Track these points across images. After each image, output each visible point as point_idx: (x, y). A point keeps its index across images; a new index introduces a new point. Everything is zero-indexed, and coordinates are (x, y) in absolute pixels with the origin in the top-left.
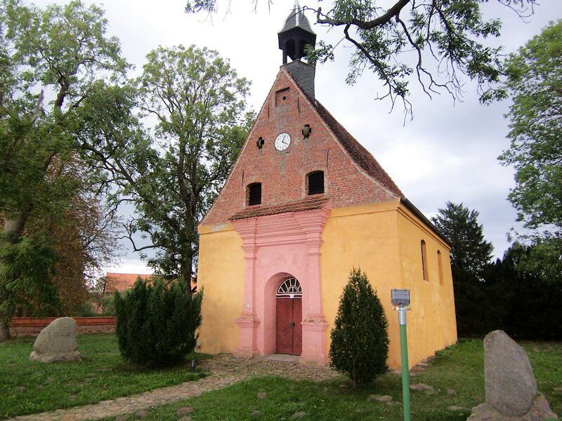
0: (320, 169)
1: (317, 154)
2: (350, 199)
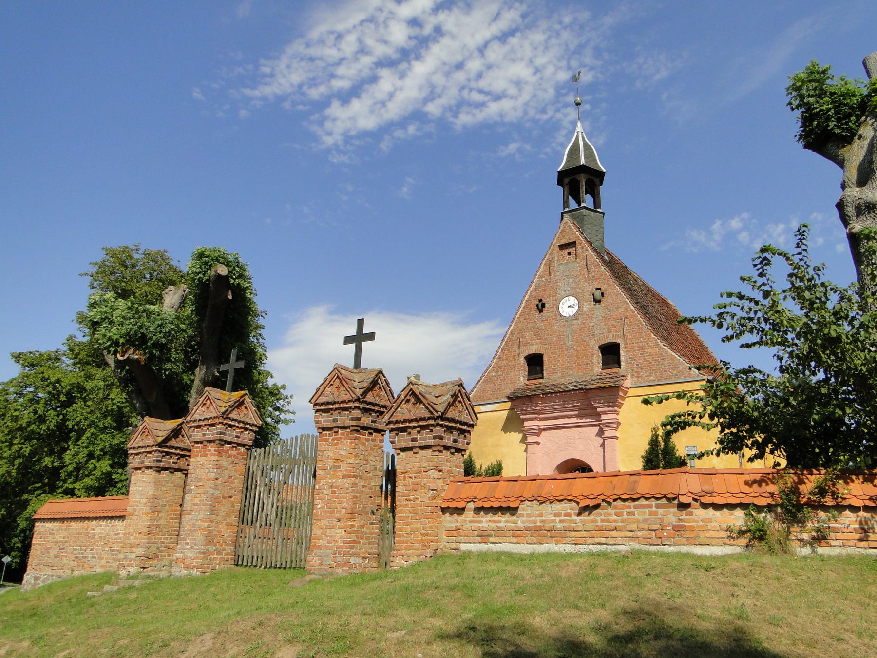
0: (614, 341)
1: (611, 323)
2: (650, 376)
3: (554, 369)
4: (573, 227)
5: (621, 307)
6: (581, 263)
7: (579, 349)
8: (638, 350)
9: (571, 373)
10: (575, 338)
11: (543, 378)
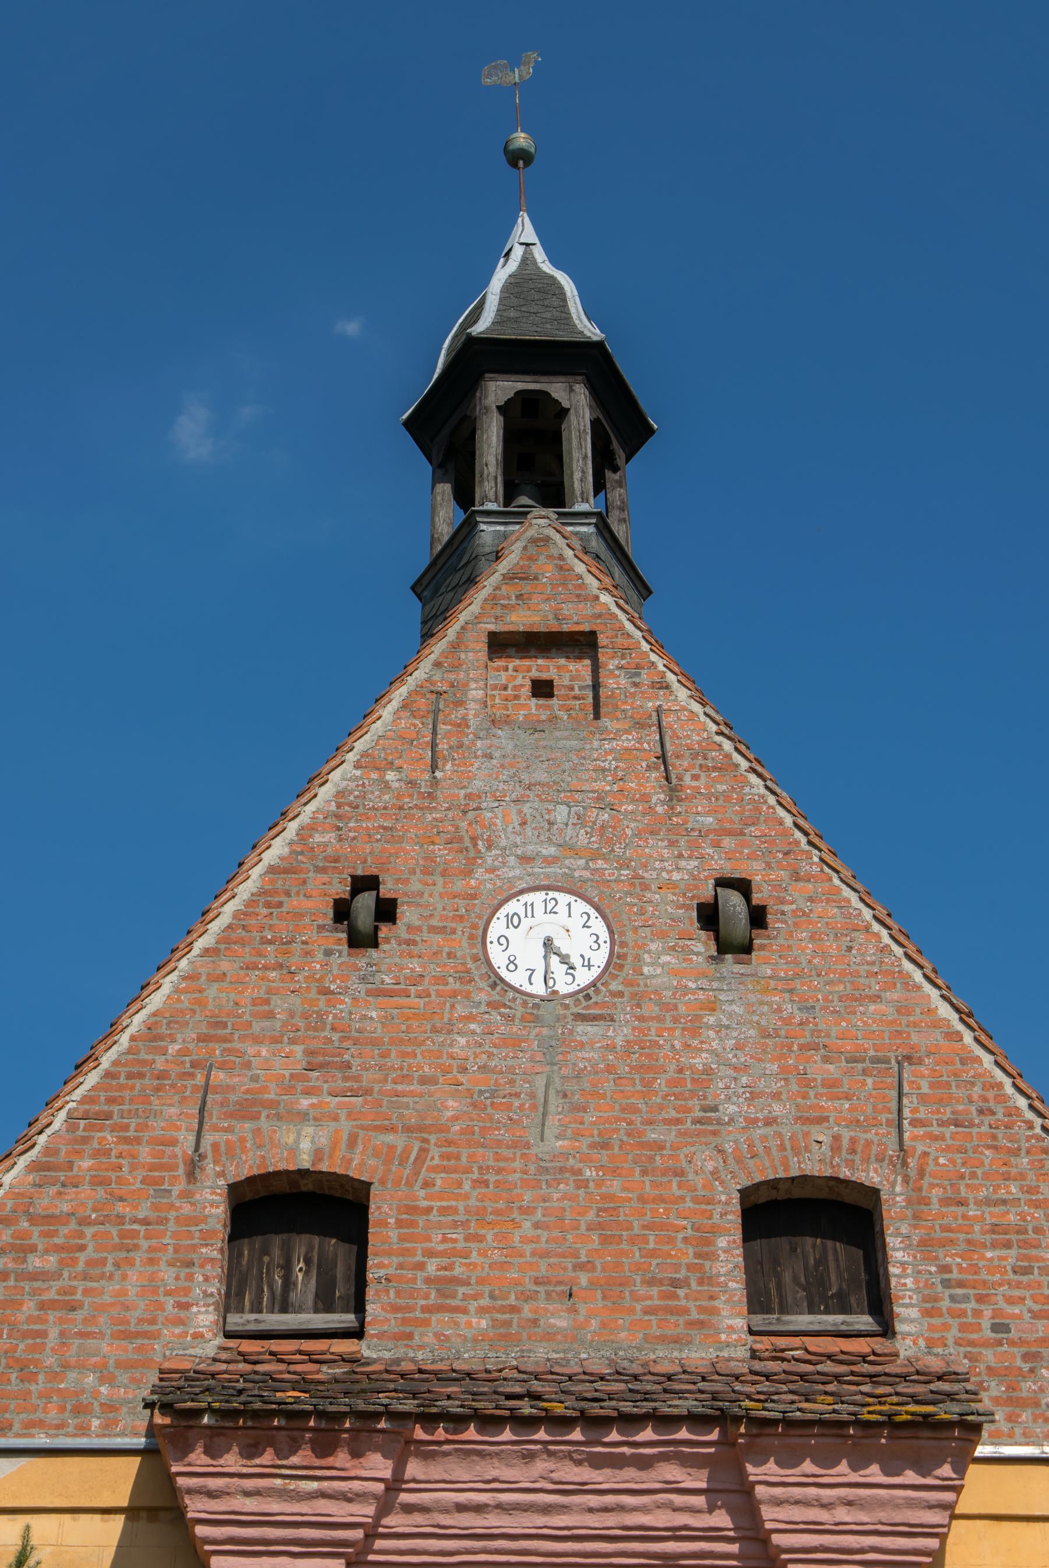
0: (845, 1173)
1: (819, 1069)
3: (445, 1284)
4: (580, 568)
5: (876, 998)
6: (628, 741)
7: (615, 1186)
8: (994, 1246)
9: (561, 1322)
10: (590, 1118)
11: (358, 1333)
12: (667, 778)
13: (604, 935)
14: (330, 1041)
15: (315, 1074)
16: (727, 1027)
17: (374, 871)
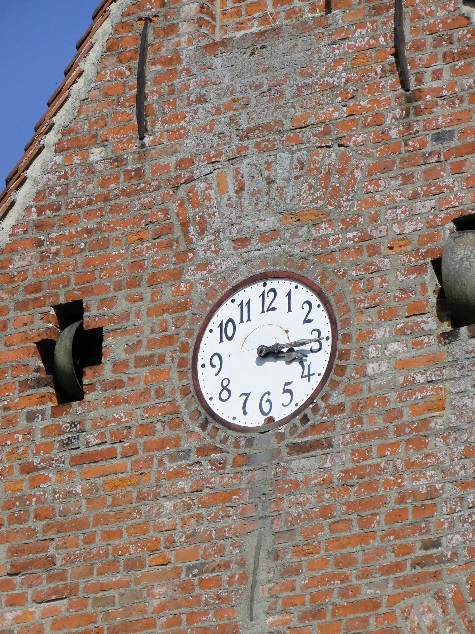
10: (300, 581)
12: (404, 84)
13: (327, 331)
14: (33, 531)
15: (18, 579)
16: (457, 429)
17: (77, 294)
